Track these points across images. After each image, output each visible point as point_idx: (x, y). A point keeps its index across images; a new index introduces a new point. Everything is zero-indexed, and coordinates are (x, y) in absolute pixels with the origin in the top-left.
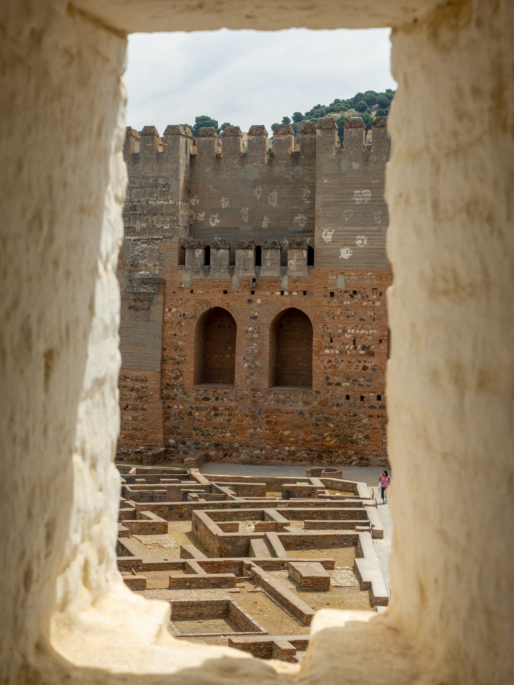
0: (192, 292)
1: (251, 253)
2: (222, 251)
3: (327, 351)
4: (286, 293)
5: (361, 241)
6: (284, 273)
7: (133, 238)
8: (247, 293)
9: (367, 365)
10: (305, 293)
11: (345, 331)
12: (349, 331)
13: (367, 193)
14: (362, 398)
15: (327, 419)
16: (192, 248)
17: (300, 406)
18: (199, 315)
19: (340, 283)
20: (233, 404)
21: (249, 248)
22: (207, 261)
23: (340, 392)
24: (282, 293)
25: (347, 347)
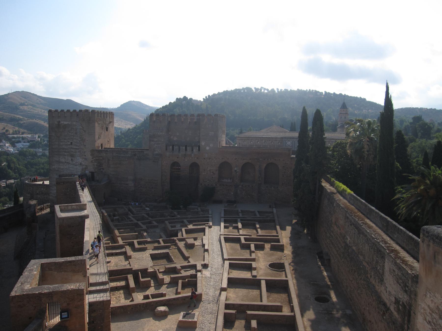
0: (169, 157)
1: (184, 148)
2: (177, 147)
3: (203, 173)
4: (193, 158)
5: (211, 145)
7: (154, 143)
9: (213, 177)
10: (198, 158)
11: (208, 168)
12: (209, 168)
22: (173, 150)
24: (192, 158)
25: (208, 172)
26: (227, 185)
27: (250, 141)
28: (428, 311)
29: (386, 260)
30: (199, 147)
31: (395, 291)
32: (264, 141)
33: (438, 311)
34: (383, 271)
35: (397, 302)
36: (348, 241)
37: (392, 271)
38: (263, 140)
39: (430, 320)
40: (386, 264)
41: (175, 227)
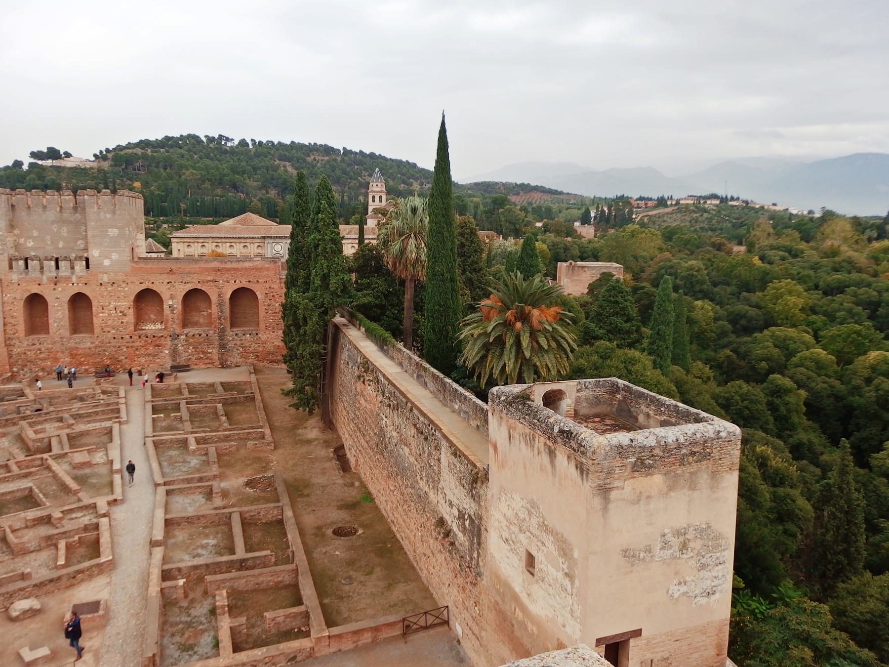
1: (53, 263)
5: (115, 256)
6: (73, 273)
8: (53, 285)
11: (110, 304)
13: (116, 231)
14: (122, 338)
15: (104, 350)
16: (16, 260)
17: (88, 345)
18: (24, 298)
19: (105, 278)
20: (50, 346)
21: (51, 260)
23: (109, 335)
26: (154, 336)
27: (201, 245)
28: (505, 522)
29: (443, 449)
30: (87, 260)
31: (458, 499)
32: (228, 245)
33: (518, 520)
34: (439, 467)
35: (461, 516)
36: (384, 422)
37: (453, 467)
38: (225, 243)
39: (508, 537)
40: (443, 455)
41: (43, 431)
